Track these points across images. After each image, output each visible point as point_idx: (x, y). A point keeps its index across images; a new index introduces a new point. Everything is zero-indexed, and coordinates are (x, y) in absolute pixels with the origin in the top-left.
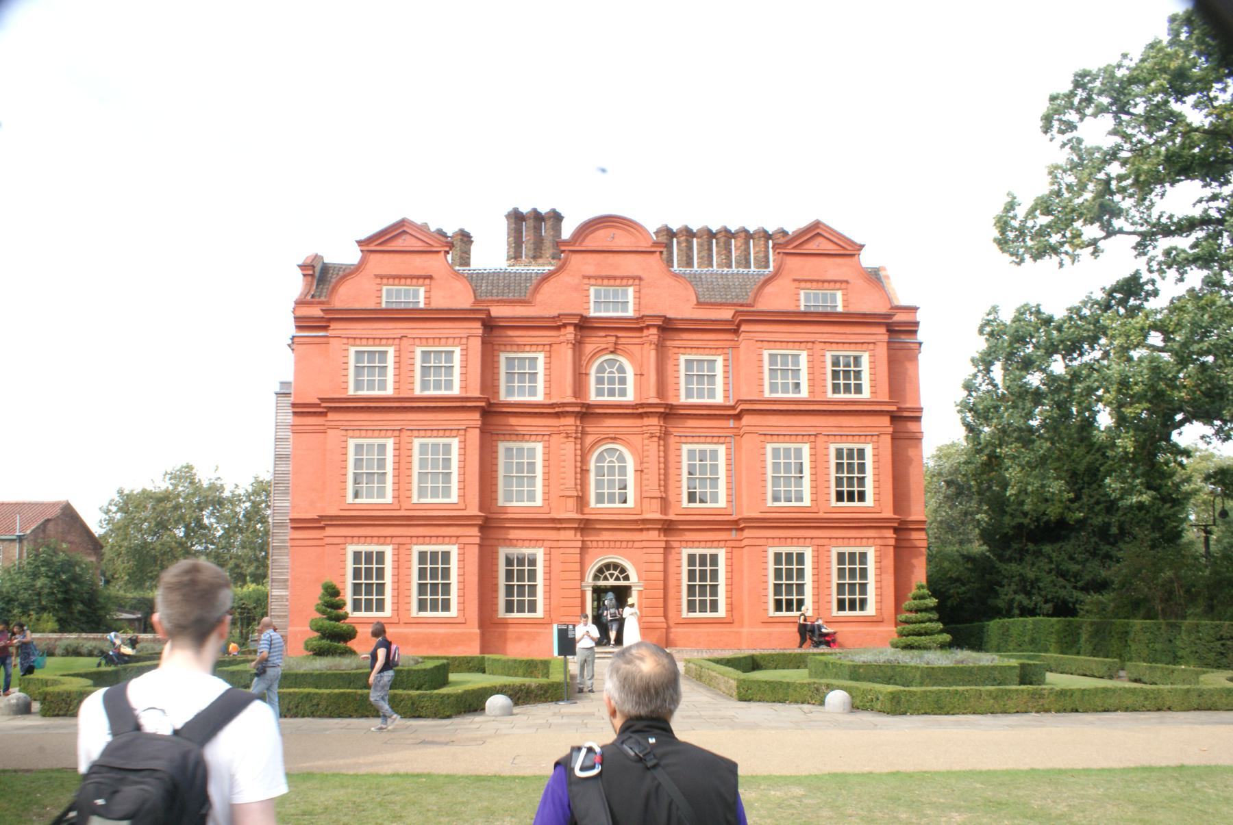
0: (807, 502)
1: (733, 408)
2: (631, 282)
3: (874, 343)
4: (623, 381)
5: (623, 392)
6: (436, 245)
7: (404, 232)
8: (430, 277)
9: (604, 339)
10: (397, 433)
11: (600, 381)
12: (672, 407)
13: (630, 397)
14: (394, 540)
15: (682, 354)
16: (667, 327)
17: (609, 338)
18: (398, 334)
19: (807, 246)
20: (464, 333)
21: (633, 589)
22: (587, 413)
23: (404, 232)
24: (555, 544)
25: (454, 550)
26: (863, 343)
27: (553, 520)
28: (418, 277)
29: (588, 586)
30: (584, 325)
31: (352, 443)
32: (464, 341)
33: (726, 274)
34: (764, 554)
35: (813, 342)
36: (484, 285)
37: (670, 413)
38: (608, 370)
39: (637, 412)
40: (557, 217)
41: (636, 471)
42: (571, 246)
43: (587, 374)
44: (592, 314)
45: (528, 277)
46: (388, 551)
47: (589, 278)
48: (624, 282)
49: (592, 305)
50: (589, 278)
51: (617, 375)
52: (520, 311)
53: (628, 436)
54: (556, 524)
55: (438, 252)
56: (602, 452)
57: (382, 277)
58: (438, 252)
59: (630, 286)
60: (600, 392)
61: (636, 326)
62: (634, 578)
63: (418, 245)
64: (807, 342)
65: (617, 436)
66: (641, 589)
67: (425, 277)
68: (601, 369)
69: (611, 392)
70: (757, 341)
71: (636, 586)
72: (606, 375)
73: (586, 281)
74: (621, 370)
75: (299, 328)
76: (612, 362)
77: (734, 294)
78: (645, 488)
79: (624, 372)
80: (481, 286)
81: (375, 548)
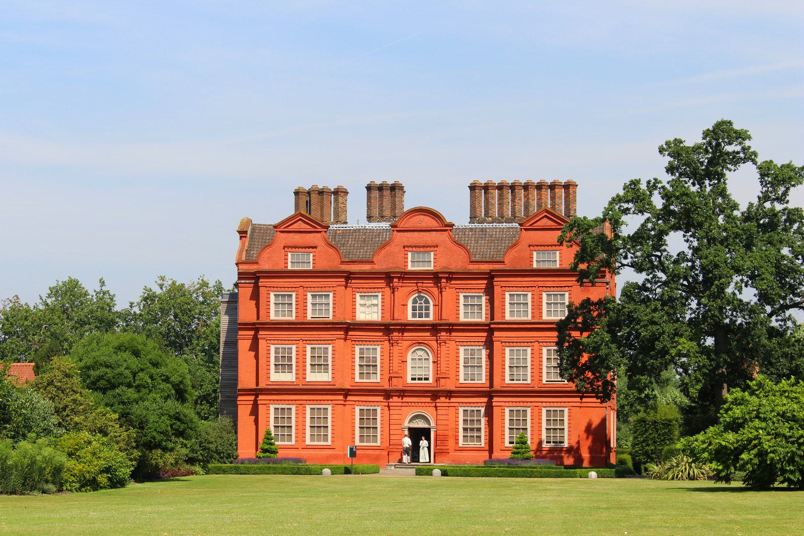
0: (529, 381)
1: (488, 325)
2: (432, 249)
3: (572, 286)
4: (427, 308)
5: (427, 315)
6: (319, 227)
7: (300, 219)
8: (316, 247)
9: (415, 284)
10: (297, 342)
11: (414, 309)
12: (453, 325)
13: (431, 318)
14: (298, 402)
15: (462, 293)
16: (451, 276)
17: (418, 284)
18: (298, 284)
19: (539, 224)
20: (335, 284)
21: (431, 430)
22: (405, 328)
23: (300, 219)
24: (386, 404)
25: (330, 408)
26: (565, 287)
27: (385, 391)
28: (309, 247)
29: (406, 428)
30: (406, 276)
31: (273, 348)
32: (334, 289)
33: (503, 228)
34: (503, 411)
35: (535, 287)
36: (350, 240)
37: (453, 328)
38: (419, 302)
39: (434, 329)
40: (395, 189)
41: (433, 362)
42: (397, 227)
43: (405, 305)
44: (410, 268)
45: (380, 232)
46: (293, 407)
47: (408, 247)
48: (428, 249)
49: (410, 264)
50: (408, 247)
51: (424, 305)
52: (366, 268)
53: (429, 342)
54: (387, 394)
55: (320, 232)
56: (414, 351)
57: (288, 247)
58: (320, 232)
59: (432, 251)
60: (414, 315)
61: (435, 277)
62: (433, 424)
63: (309, 228)
64: (532, 287)
65: (423, 342)
66: (436, 430)
67: (313, 247)
68: (415, 301)
69: (421, 316)
70: (502, 287)
71: (433, 428)
72: (418, 305)
73: (406, 249)
74: (427, 302)
75: (239, 278)
76: (420, 298)
77: (503, 245)
78: (439, 372)
79: (429, 303)
80: (348, 241)
81: (286, 406)
